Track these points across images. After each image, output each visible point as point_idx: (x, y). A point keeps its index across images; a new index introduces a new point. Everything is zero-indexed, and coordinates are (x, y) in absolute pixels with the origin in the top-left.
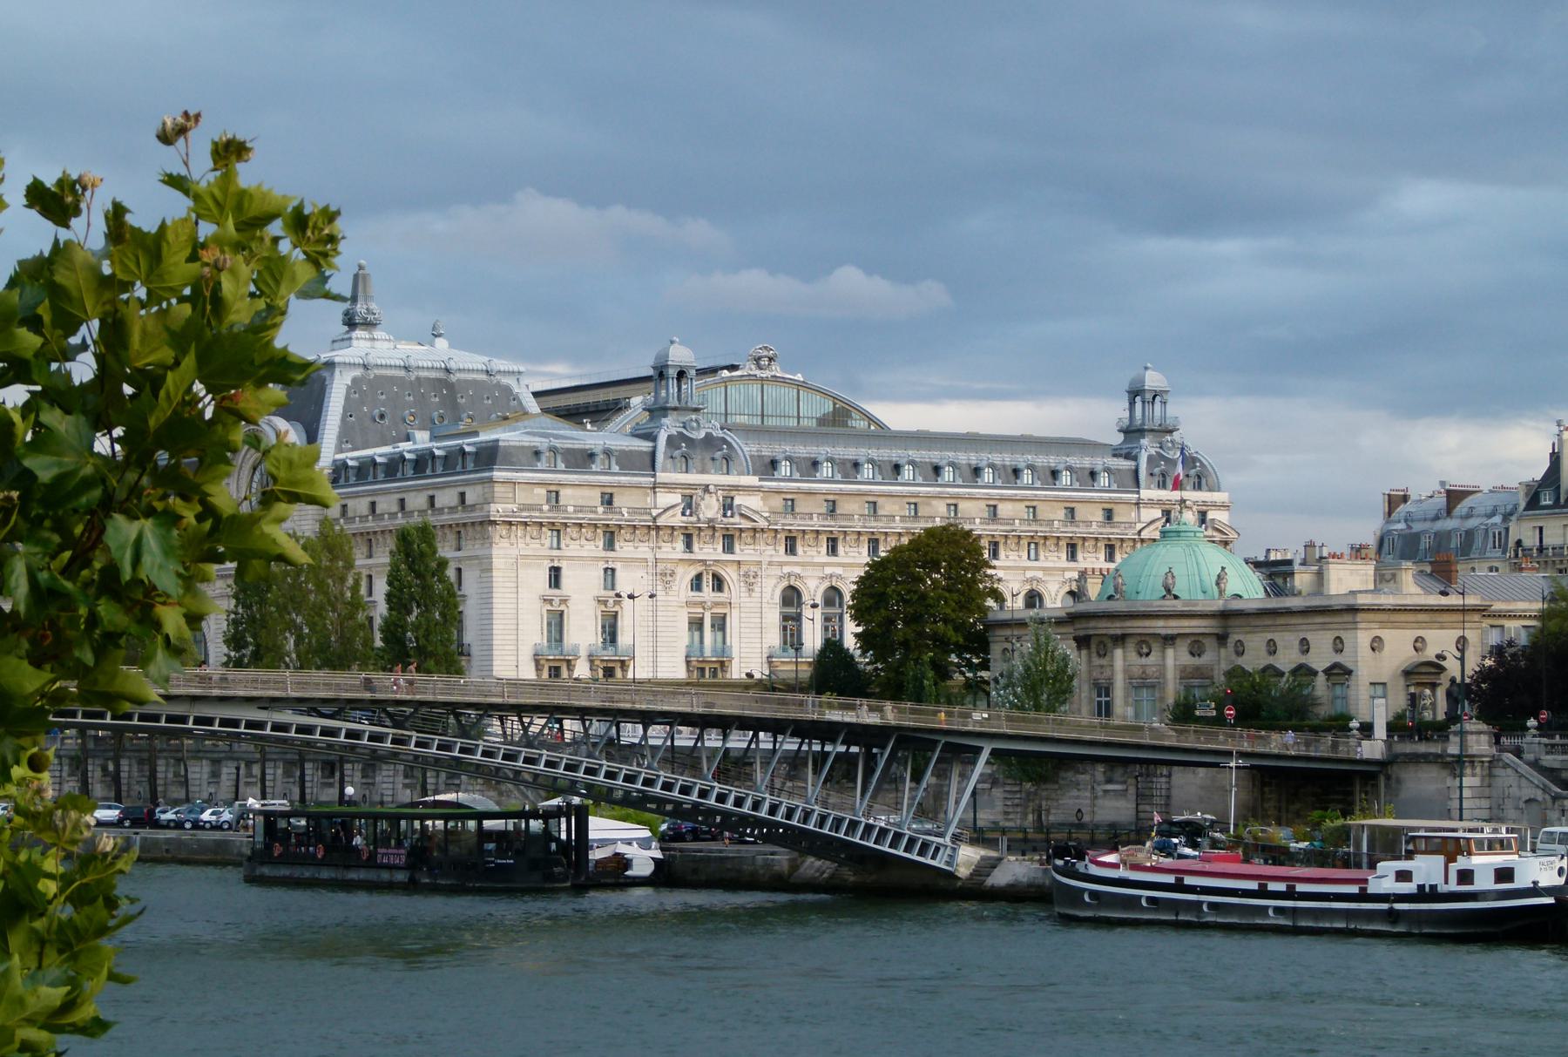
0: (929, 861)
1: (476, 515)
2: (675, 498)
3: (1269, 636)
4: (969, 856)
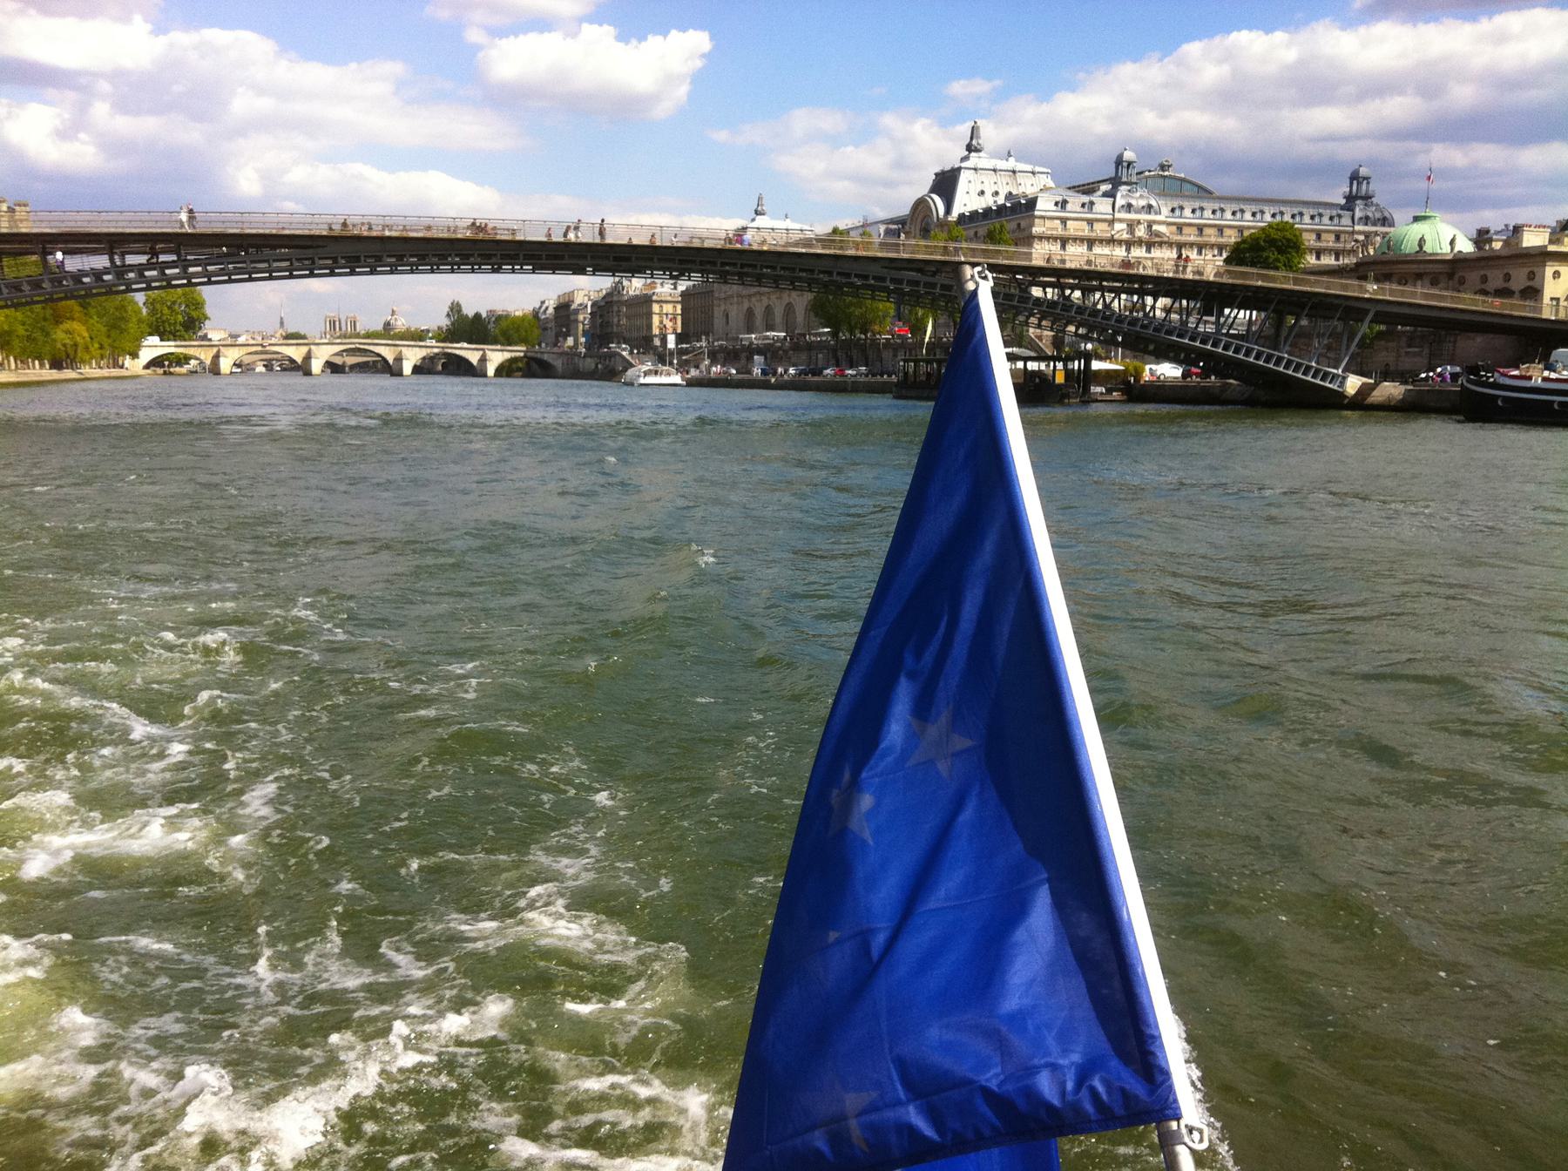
0: (1327, 385)
1: (1026, 234)
2: (1124, 226)
3: (1482, 273)
4: (1353, 384)
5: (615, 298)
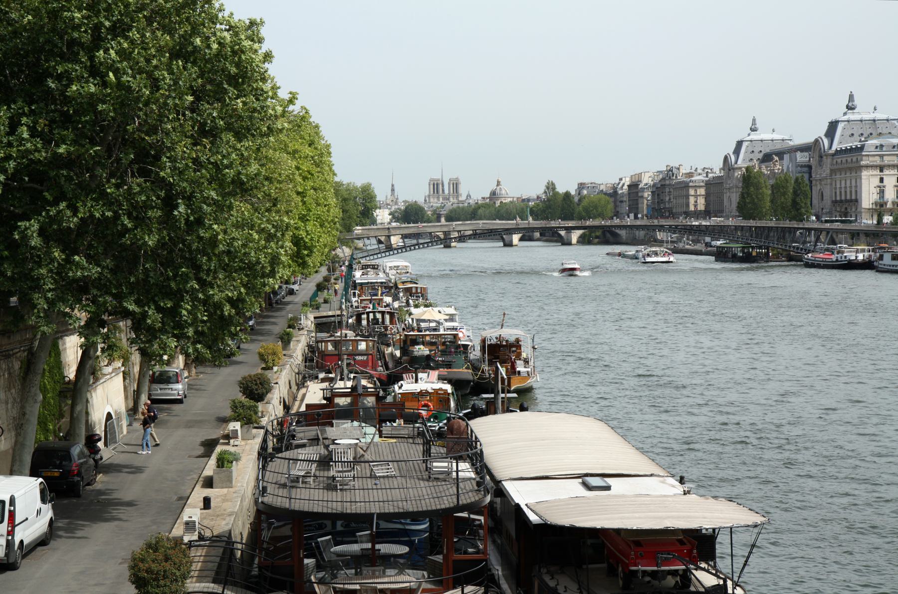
5: (667, 182)
